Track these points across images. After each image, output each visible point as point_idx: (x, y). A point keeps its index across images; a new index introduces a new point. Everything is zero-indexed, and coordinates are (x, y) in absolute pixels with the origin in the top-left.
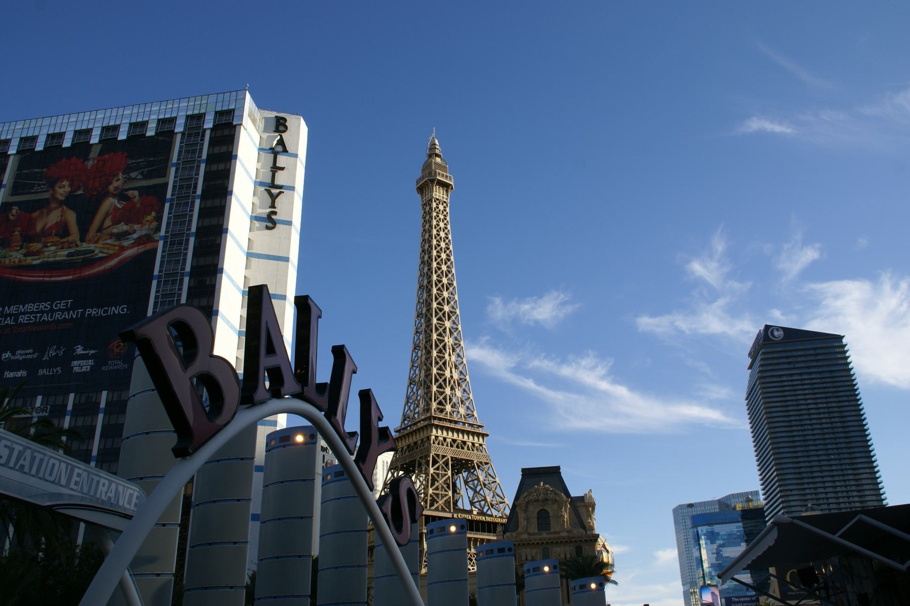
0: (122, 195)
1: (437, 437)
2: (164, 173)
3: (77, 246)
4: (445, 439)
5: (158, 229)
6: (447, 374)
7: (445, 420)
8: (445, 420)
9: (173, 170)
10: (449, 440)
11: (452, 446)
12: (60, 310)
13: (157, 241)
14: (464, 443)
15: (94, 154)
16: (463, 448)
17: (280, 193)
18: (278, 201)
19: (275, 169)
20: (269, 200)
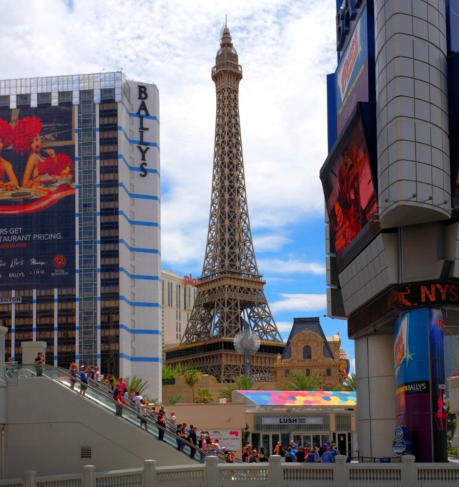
0: (43, 153)
1: (230, 286)
2: (69, 137)
3: (17, 189)
4: (235, 287)
5: (73, 180)
6: (237, 238)
7: (235, 273)
8: (235, 273)
9: (76, 135)
10: (238, 288)
11: (240, 292)
12: (14, 234)
13: (74, 189)
14: (249, 289)
15: (15, 116)
16: (247, 293)
17: (147, 149)
18: (147, 155)
19: (142, 129)
20: (140, 155)
